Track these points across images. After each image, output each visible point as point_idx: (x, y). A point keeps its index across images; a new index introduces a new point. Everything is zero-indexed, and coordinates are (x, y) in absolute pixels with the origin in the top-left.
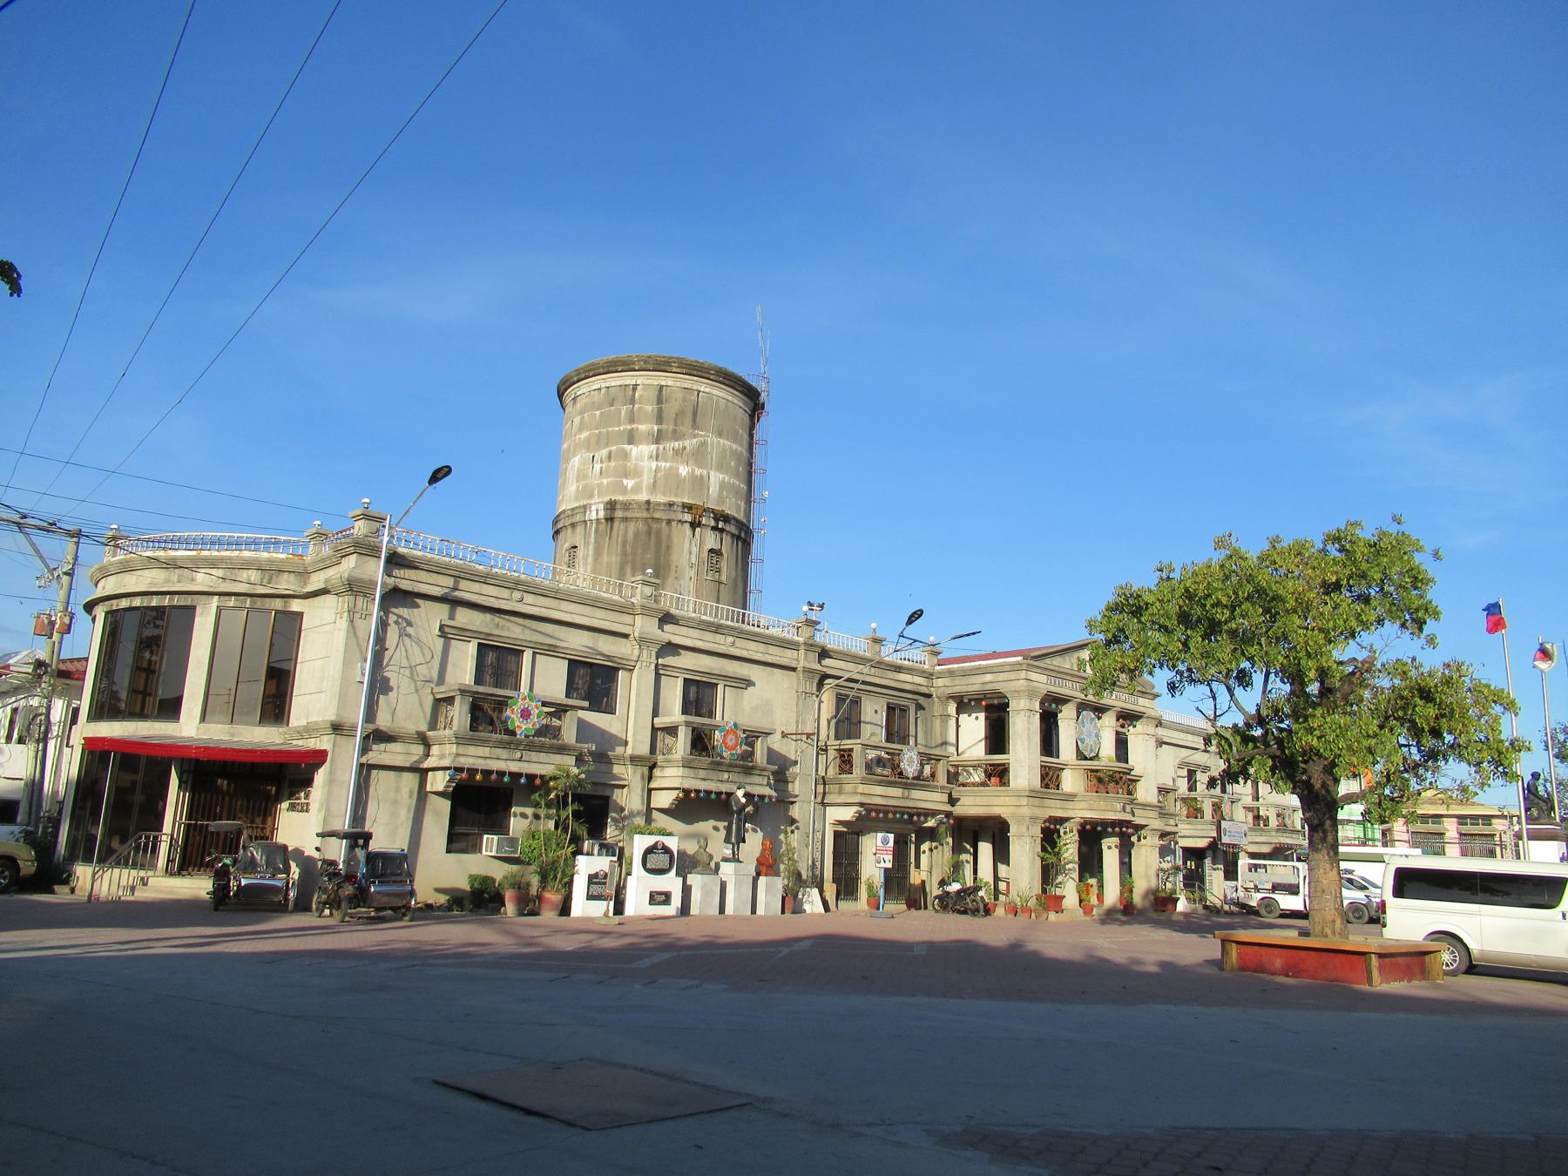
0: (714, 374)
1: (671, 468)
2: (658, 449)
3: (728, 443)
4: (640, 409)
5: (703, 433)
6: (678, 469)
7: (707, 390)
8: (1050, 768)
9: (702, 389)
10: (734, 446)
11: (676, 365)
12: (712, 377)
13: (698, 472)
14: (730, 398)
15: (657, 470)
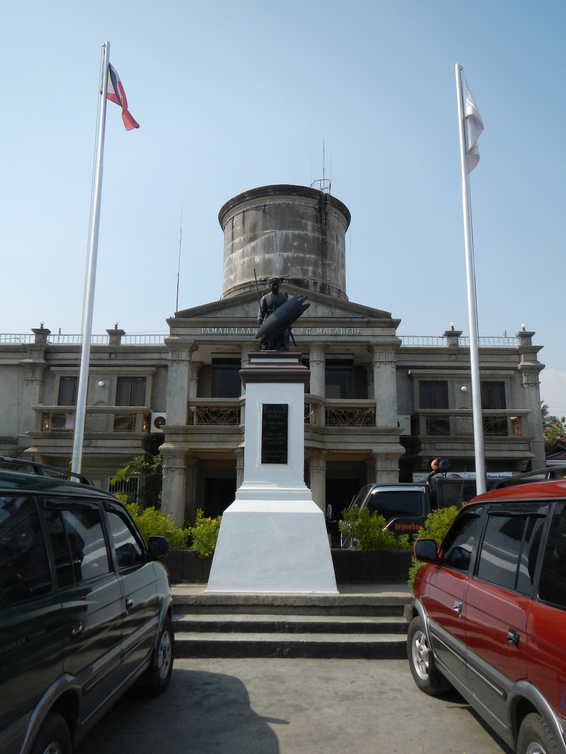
0: (272, 191)
1: (251, 259)
2: (244, 250)
3: (290, 232)
4: (236, 229)
5: (269, 231)
6: (254, 258)
7: (271, 203)
8: (217, 407)
9: (268, 203)
10: (297, 232)
11: (247, 195)
12: (270, 194)
13: (267, 256)
14: (287, 202)
15: (244, 263)
